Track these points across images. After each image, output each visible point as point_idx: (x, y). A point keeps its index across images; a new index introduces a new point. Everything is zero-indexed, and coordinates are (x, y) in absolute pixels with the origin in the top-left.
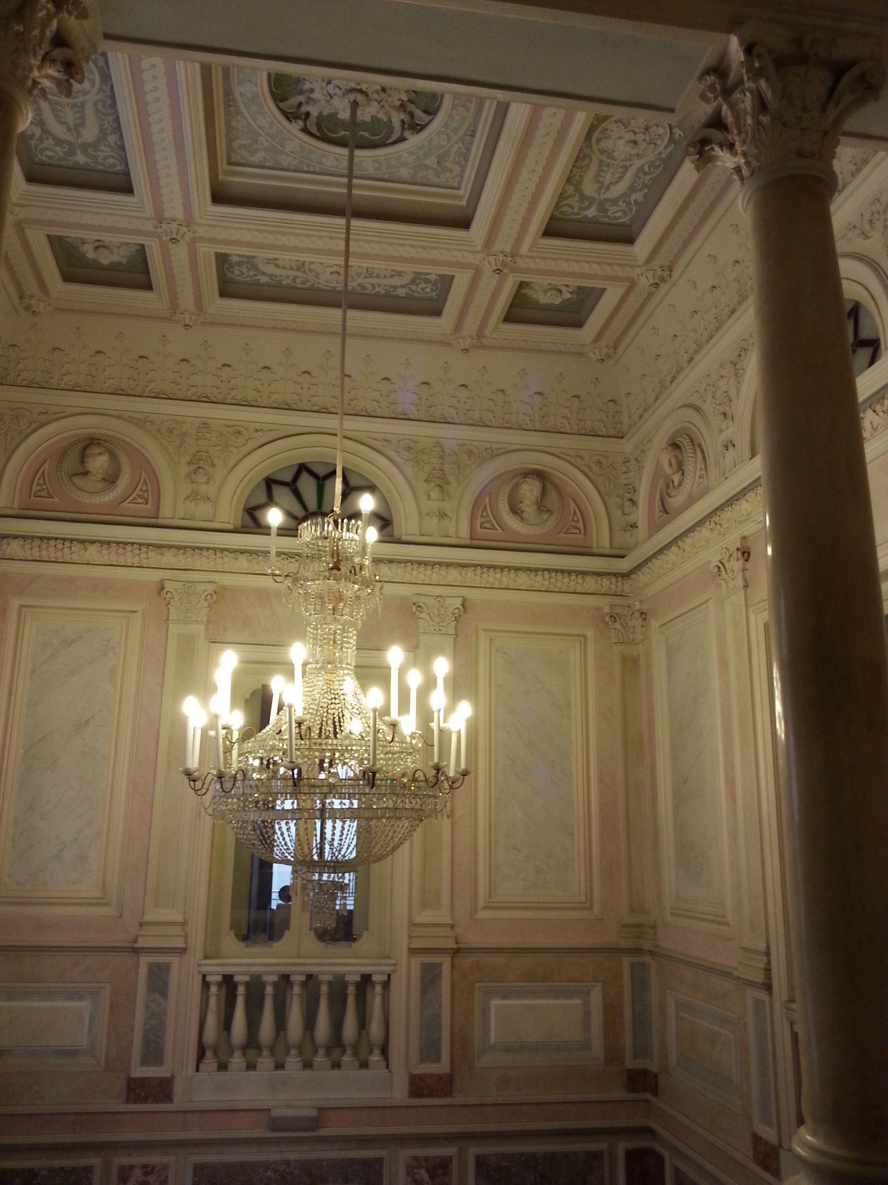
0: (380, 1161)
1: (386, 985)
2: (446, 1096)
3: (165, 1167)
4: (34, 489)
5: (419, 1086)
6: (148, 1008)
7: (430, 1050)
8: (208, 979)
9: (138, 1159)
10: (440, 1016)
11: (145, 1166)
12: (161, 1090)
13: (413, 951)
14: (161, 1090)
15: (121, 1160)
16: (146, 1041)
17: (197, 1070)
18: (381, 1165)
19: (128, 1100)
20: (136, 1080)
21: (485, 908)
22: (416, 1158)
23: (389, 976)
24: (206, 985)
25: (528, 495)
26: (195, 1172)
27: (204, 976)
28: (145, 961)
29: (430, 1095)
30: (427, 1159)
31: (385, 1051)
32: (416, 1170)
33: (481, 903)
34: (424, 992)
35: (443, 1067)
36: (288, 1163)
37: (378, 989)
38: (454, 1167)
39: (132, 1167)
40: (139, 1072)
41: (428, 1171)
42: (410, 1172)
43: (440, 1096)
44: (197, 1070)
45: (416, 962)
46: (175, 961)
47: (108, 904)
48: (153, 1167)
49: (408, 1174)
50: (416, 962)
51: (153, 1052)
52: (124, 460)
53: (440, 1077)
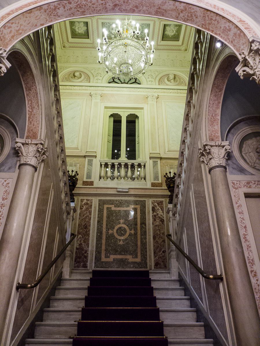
0: (145, 201)
1: (144, 166)
2: (161, 187)
3: (92, 200)
4: (64, 80)
5: (153, 185)
6: (88, 168)
7: (156, 178)
8: (101, 163)
9: (85, 198)
10: (158, 171)
11: (87, 199)
12: (92, 183)
13: (151, 158)
14: (92, 183)
15: (81, 198)
16: (87, 174)
17: (99, 181)
18: (145, 202)
19: (83, 185)
20: (85, 181)
21: (167, 152)
22: (154, 201)
23: (145, 164)
24: (101, 165)
25: (171, 77)
26: (99, 201)
27: (101, 163)
28: (87, 159)
29: (157, 187)
30: (157, 201)
31: (145, 179)
32: (154, 203)
33: (167, 151)
34: (154, 167)
35: (160, 181)
36: (122, 200)
37: (143, 167)
38: (164, 203)
39: (84, 199)
40: (85, 180)
41: (157, 203)
42: (152, 203)
43: (159, 187)
44: (99, 181)
45: (151, 161)
46: (94, 159)
47: (79, 149)
48: (89, 200)
49: (152, 204)
50: (151, 161)
51: (89, 176)
52: (82, 74)
53: (159, 183)
